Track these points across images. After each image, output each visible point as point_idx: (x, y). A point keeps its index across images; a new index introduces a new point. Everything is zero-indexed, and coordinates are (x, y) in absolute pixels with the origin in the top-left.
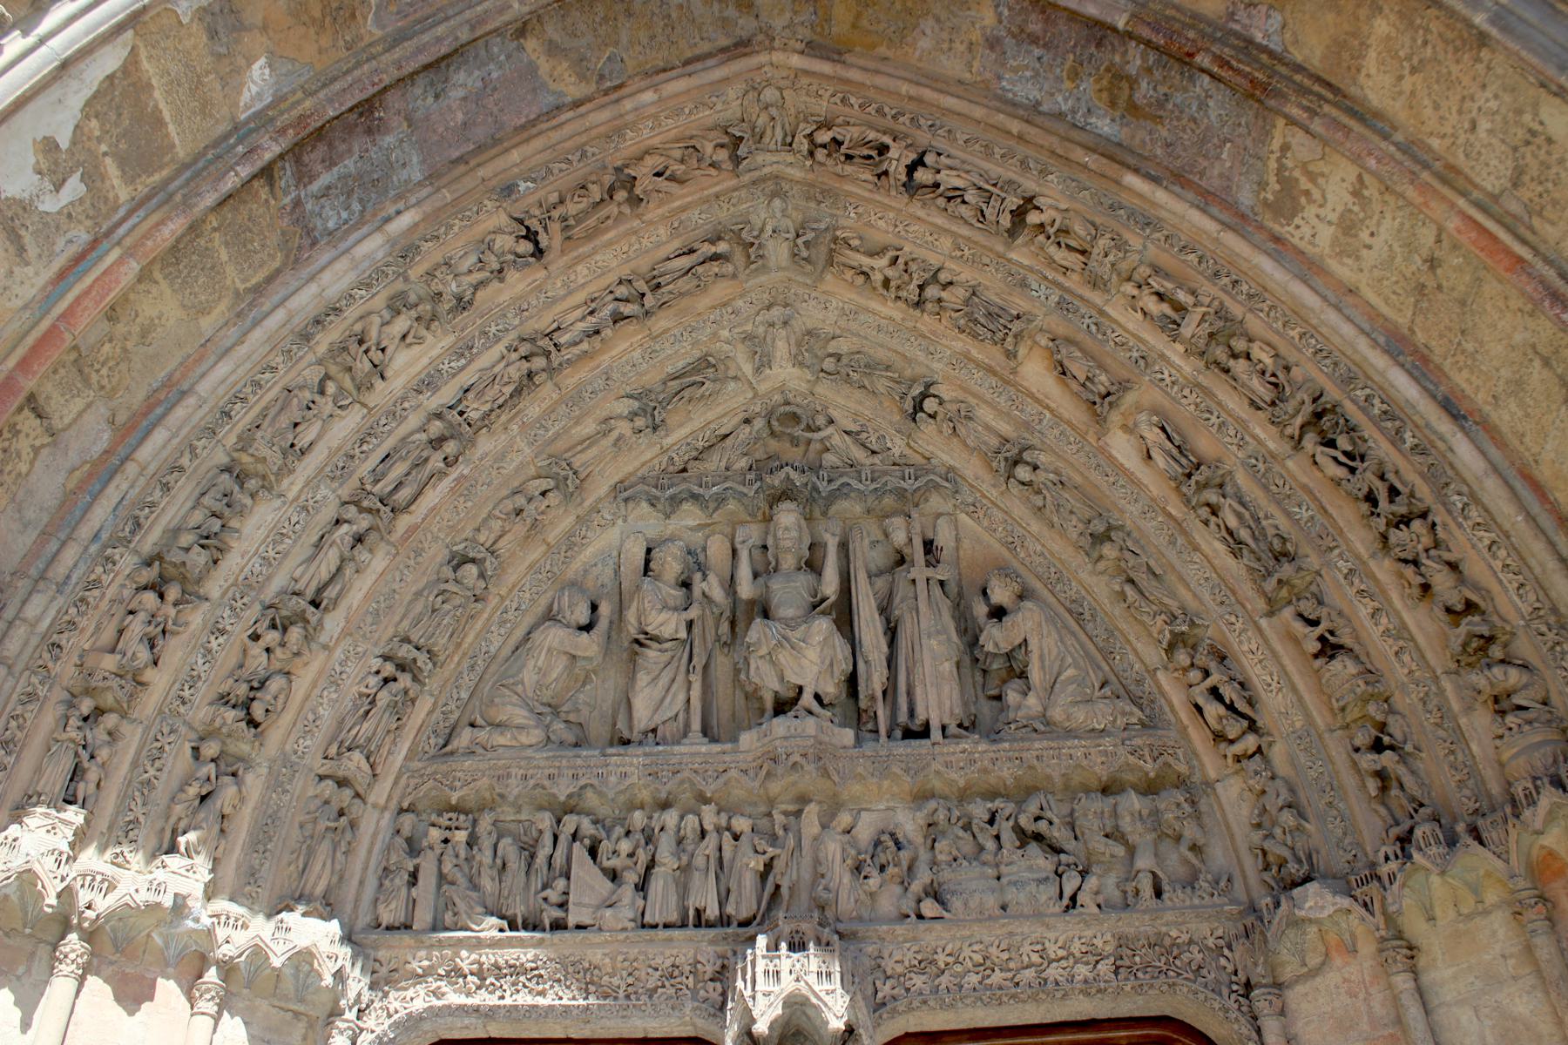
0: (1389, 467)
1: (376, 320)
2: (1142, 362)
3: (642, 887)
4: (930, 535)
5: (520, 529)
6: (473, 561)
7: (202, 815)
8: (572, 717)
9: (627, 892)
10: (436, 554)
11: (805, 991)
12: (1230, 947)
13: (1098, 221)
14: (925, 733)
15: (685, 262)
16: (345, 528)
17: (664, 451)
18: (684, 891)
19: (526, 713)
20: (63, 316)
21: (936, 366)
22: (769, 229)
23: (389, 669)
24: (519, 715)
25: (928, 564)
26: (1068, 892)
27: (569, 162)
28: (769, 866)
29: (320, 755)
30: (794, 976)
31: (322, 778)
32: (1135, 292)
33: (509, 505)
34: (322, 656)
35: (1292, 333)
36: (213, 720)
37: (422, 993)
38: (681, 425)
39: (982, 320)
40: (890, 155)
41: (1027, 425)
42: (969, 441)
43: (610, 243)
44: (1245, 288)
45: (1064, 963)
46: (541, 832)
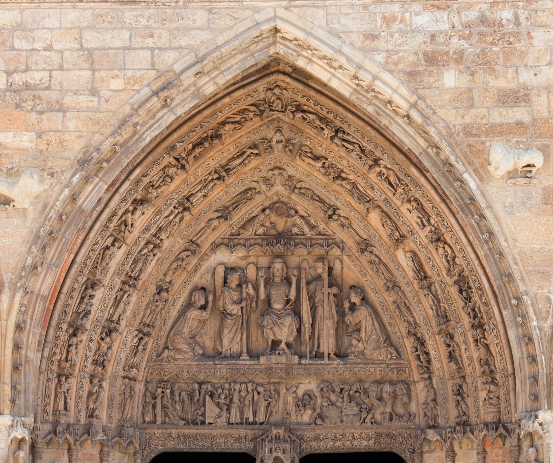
0: (477, 305)
3: (228, 410)
4: (332, 265)
7: (97, 404)
9: (224, 414)
10: (153, 289)
11: (280, 455)
12: (411, 438)
13: (401, 177)
15: (240, 160)
17: (230, 226)
18: (242, 413)
19: (187, 347)
20: (57, 281)
22: (274, 140)
24: (185, 348)
26: (363, 418)
27: (195, 131)
28: (269, 404)
31: (124, 378)
33: (175, 265)
36: (94, 371)
38: (237, 215)
40: (324, 132)
41: (369, 236)
43: (211, 157)
45: (359, 440)
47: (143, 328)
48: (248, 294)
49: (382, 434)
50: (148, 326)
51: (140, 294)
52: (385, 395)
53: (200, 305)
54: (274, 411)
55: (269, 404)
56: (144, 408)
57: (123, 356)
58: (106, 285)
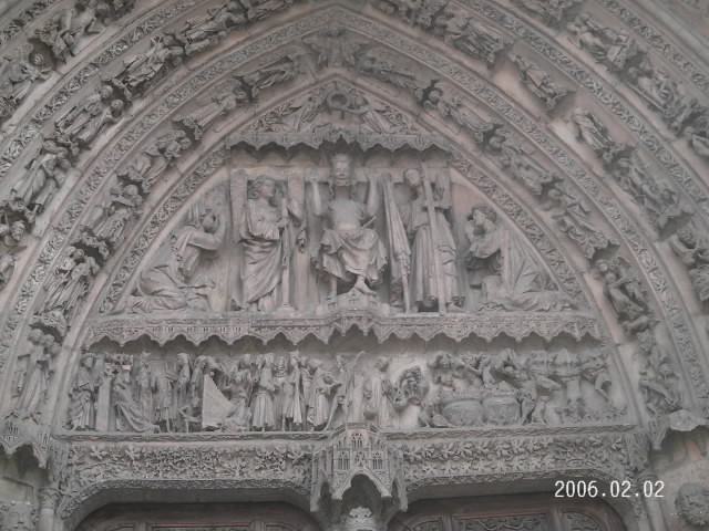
1: (69, 15)
2: (579, 77)
4: (433, 180)
5: (162, 163)
6: (134, 183)
8: (201, 291)
14: (435, 307)
16: (48, 157)
17: (255, 115)
21: (438, 71)
23: (80, 252)
25: (435, 200)
28: (334, 390)
29: (33, 312)
30: (358, 463)
31: (34, 327)
32: (577, 29)
34: (35, 243)
35: (679, 63)
37: (102, 471)
39: (474, 42)
42: (459, 121)
44: (650, 31)
45: (522, 456)
46: (181, 367)
47: (85, 240)
48: (291, 215)
49: (568, 443)
50: (99, 241)
51: (85, 178)
52: (562, 372)
53: (202, 228)
54: (345, 402)
55: (334, 390)
56: (73, 401)
57: (37, 286)
58: (9, 132)
